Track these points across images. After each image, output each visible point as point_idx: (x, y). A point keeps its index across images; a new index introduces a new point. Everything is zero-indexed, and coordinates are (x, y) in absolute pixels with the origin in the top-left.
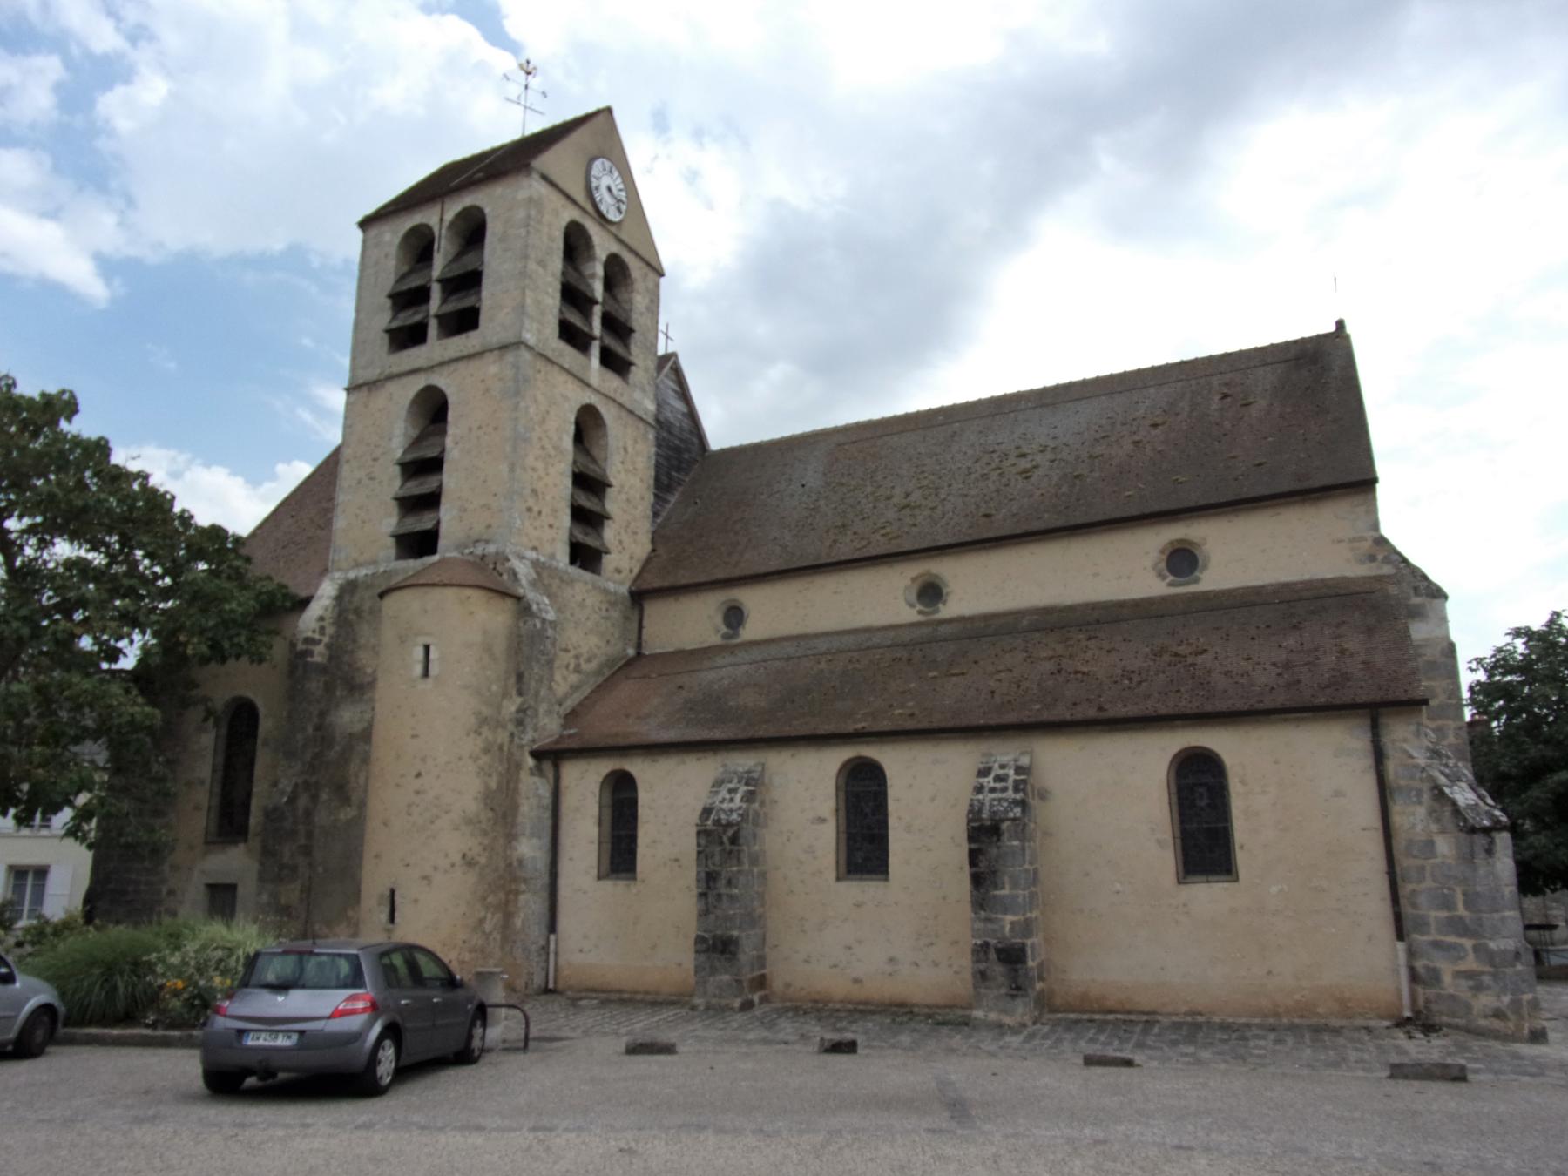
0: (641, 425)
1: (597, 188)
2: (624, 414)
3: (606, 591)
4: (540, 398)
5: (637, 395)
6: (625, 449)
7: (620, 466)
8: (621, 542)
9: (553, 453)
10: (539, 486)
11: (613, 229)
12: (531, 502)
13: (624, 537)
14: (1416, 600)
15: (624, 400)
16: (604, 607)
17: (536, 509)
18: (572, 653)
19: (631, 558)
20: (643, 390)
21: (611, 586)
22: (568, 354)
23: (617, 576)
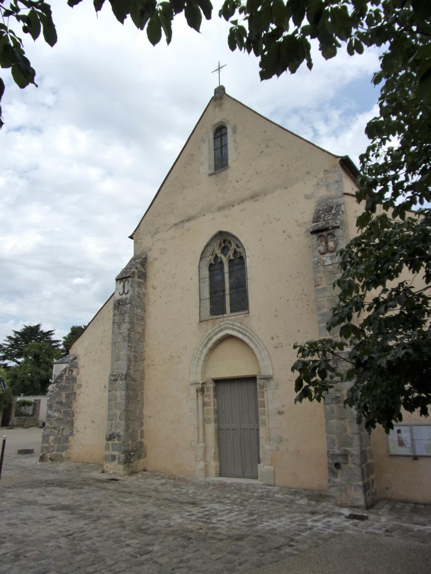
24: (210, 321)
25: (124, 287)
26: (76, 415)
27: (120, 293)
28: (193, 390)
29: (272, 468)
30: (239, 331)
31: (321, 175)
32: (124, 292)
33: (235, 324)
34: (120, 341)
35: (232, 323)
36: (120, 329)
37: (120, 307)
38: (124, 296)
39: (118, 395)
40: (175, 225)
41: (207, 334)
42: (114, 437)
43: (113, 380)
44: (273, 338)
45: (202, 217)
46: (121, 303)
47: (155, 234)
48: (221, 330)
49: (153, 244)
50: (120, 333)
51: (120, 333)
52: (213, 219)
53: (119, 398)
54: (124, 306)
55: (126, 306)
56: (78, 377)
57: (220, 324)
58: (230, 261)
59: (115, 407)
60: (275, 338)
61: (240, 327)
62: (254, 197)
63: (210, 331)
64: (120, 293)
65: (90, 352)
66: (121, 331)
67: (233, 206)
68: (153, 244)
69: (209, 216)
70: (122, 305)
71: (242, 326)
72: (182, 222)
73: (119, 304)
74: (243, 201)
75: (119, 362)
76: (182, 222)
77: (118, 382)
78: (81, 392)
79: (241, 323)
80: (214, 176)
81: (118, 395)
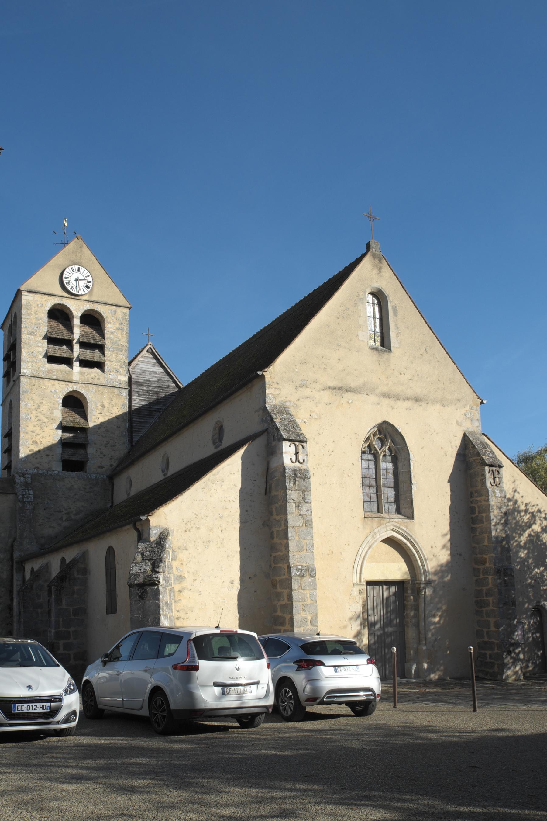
0: (116, 390)
1: (68, 283)
2: (101, 388)
4: (34, 396)
5: (113, 376)
6: (103, 406)
7: (99, 415)
8: (102, 453)
9: (46, 420)
15: (102, 381)
19: (111, 459)
20: (117, 372)
21: (93, 477)
23: (100, 470)
24: (376, 519)
25: (297, 453)
27: (291, 459)
30: (403, 536)
31: (468, 408)
32: (297, 460)
33: (401, 527)
34: (301, 525)
35: (398, 525)
36: (300, 510)
37: (297, 479)
40: (330, 388)
43: (299, 575)
44: (432, 547)
45: (366, 396)
46: (299, 475)
49: (298, 400)
50: (300, 515)
51: (300, 515)
52: (378, 404)
53: (309, 599)
54: (304, 480)
56: (175, 564)
57: (387, 524)
60: (434, 547)
61: (405, 532)
62: (417, 400)
64: (291, 459)
65: (199, 528)
66: (302, 513)
67: (399, 400)
68: (298, 400)
69: (373, 398)
70: (300, 478)
71: (407, 531)
72: (340, 389)
73: (295, 474)
77: (305, 578)
79: (407, 527)
80: (375, 352)
81: (308, 596)
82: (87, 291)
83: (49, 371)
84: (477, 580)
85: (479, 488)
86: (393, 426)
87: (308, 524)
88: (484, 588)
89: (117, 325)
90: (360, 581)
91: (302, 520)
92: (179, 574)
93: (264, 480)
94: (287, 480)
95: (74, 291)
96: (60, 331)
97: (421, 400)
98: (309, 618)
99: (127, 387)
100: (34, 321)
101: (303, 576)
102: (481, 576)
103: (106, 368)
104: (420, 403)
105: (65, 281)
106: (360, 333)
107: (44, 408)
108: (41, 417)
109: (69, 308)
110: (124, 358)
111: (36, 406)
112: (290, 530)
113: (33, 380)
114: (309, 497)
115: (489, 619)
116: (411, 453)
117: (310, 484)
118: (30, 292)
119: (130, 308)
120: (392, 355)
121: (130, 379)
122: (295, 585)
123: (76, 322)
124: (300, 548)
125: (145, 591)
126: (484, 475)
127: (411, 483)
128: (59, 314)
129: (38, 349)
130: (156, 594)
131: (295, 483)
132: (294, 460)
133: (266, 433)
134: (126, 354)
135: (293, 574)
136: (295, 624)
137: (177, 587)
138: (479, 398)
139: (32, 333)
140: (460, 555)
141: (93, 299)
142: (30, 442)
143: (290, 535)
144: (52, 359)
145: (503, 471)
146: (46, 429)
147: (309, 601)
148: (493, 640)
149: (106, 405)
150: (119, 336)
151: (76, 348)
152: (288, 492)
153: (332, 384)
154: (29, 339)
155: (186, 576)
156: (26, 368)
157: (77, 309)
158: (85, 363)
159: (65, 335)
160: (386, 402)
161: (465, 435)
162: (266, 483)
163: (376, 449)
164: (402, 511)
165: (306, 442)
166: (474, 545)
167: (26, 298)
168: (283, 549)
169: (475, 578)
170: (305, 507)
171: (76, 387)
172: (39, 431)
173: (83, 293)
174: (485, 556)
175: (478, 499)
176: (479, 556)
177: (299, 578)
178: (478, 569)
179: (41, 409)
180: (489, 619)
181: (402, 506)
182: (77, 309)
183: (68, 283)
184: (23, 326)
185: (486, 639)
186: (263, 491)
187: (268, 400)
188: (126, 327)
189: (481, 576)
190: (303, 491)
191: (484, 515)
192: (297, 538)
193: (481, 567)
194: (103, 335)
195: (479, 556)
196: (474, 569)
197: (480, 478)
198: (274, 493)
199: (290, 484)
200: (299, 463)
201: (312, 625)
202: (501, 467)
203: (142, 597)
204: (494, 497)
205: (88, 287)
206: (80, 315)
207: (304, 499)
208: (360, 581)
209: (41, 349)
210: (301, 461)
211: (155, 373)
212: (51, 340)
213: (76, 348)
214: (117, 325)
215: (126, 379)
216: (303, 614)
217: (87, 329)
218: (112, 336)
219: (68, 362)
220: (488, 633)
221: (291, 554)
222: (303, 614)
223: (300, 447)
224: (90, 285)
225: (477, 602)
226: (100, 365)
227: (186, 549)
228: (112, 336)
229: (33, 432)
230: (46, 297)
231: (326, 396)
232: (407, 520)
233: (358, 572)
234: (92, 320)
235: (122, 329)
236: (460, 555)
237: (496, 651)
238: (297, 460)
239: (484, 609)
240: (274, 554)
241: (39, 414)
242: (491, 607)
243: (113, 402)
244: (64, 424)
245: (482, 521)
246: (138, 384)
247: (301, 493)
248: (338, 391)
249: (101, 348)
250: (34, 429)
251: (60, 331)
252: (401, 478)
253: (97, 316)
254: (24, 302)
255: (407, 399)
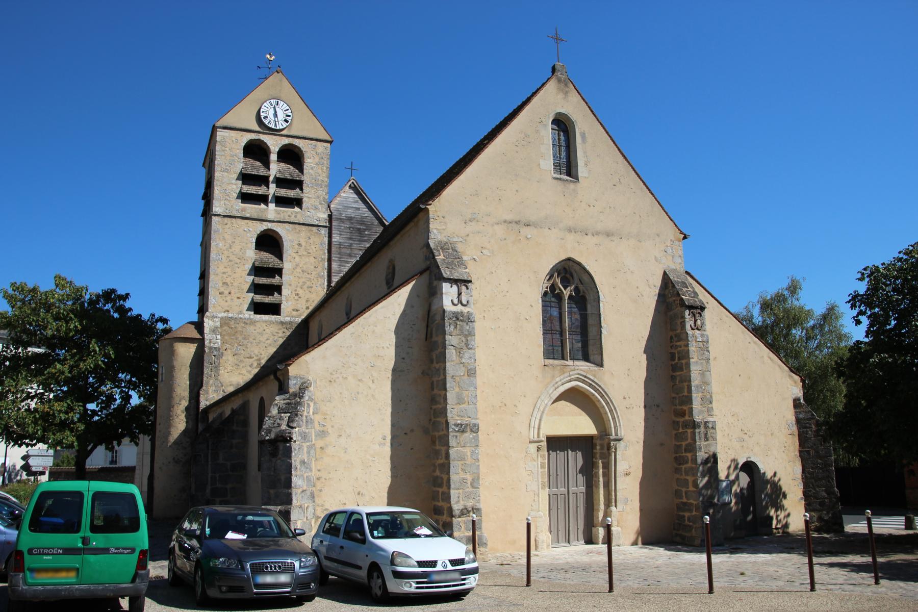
2: (297, 226)
3: (282, 323)
4: (226, 236)
6: (300, 245)
7: (295, 255)
9: (238, 261)
10: (228, 280)
11: (283, 133)
12: (222, 290)
13: (301, 292)
14: (435, 283)
16: (281, 332)
17: (226, 292)
18: (255, 358)
20: (316, 208)
22: (251, 209)
25: (460, 294)
26: (319, 485)
28: (533, 448)
29: (619, 529)
30: (590, 385)
36: (461, 358)
38: (459, 308)
39: (469, 454)
40: (505, 222)
41: (554, 382)
42: (469, 512)
45: (547, 229)
47: (470, 221)
48: (570, 381)
55: (470, 324)
56: (317, 418)
58: (570, 297)
59: (463, 470)
62: (608, 234)
63: (558, 379)
65: (346, 378)
66: (463, 361)
72: (517, 223)
74: (597, 233)
75: (462, 406)
76: (516, 223)
77: (466, 435)
78: (327, 446)
79: (595, 376)
81: (469, 454)
82: (285, 125)
83: (243, 210)
84: (676, 435)
85: (678, 331)
86: (579, 264)
87: (471, 373)
88: (684, 444)
89: (317, 160)
90: (538, 436)
91: (463, 369)
92: (321, 429)
93: (424, 325)
94: (447, 324)
95: (272, 126)
96: (256, 168)
97: (612, 235)
98: (469, 478)
99: (327, 224)
100: (228, 158)
101: (463, 432)
102: (681, 430)
103: (304, 205)
104: (612, 238)
105: (263, 115)
106: (542, 162)
107: (236, 248)
108: (232, 257)
109: (265, 144)
110: (323, 193)
111: (228, 246)
112: (449, 379)
113: (226, 220)
114: (473, 343)
115: (688, 478)
116: (600, 294)
117: (473, 328)
118: (225, 128)
119: (331, 142)
120: (579, 185)
121: (330, 216)
122: (452, 442)
123: (274, 157)
124: (460, 401)
125: (277, 448)
126: (683, 317)
127: (601, 327)
128: (256, 151)
129: (230, 187)
130: (288, 452)
131: (456, 327)
132: (456, 301)
133: (428, 272)
134: (326, 190)
135: (451, 430)
136: (452, 486)
137: (319, 443)
138: (681, 233)
139: (226, 170)
140: (658, 406)
141: (291, 133)
142: (221, 284)
143: (448, 385)
144: (245, 198)
145: (706, 313)
146: (237, 270)
147: (469, 461)
148: (691, 501)
149: (303, 244)
150: (320, 171)
151: (273, 186)
152: (448, 337)
153: (509, 217)
154: (223, 177)
155: (330, 431)
156: (217, 208)
157: (274, 144)
158: (281, 201)
159: (262, 172)
160: (571, 237)
161: (665, 273)
162: (427, 326)
163: (560, 289)
164: (591, 358)
165: (470, 281)
166: (674, 395)
167: (220, 134)
168: (442, 401)
169: (675, 432)
170: (467, 354)
171: (270, 226)
172: (230, 273)
173: (281, 127)
174: (685, 408)
175: (678, 344)
176: (679, 407)
177: (457, 434)
178: (678, 422)
179: (233, 249)
180: (688, 478)
181: (590, 352)
182: (274, 144)
183: (266, 117)
184: (216, 162)
185: (685, 500)
186: (424, 336)
187: (432, 236)
188: (326, 162)
189: (681, 430)
190: (466, 336)
191: (683, 362)
192: (457, 389)
193: (681, 420)
194: (301, 170)
195: (679, 407)
196: (674, 422)
197: (679, 321)
198: (435, 339)
199: (449, 329)
200: (462, 305)
201: (473, 487)
202: (703, 308)
203: (274, 454)
204: (694, 343)
205: (286, 121)
206: (277, 150)
207: (467, 345)
208: (538, 436)
209: (234, 187)
210: (464, 302)
211: (358, 209)
212: (246, 178)
213: (273, 186)
214: (317, 160)
215: (325, 216)
216: (462, 475)
217: (284, 166)
218: (311, 171)
219: (263, 199)
220: (686, 493)
221: (449, 407)
222: (462, 475)
223: (464, 288)
224: (289, 119)
225: (676, 459)
226: (298, 202)
227: (330, 401)
228: (311, 171)
229: (224, 273)
230: (241, 133)
231: (500, 230)
232: (596, 368)
233: (536, 426)
234: (292, 155)
235: (323, 164)
236: (658, 406)
237: (694, 513)
238: (460, 302)
239: (683, 467)
240: (434, 407)
241: (230, 255)
242: (689, 465)
243: (311, 241)
244: (257, 264)
245: (681, 369)
246: (341, 220)
247: (463, 339)
248: (514, 225)
249: (299, 184)
250: (225, 270)
251: (256, 168)
252: (591, 321)
253: (296, 150)
254: (218, 138)
255: (597, 234)
